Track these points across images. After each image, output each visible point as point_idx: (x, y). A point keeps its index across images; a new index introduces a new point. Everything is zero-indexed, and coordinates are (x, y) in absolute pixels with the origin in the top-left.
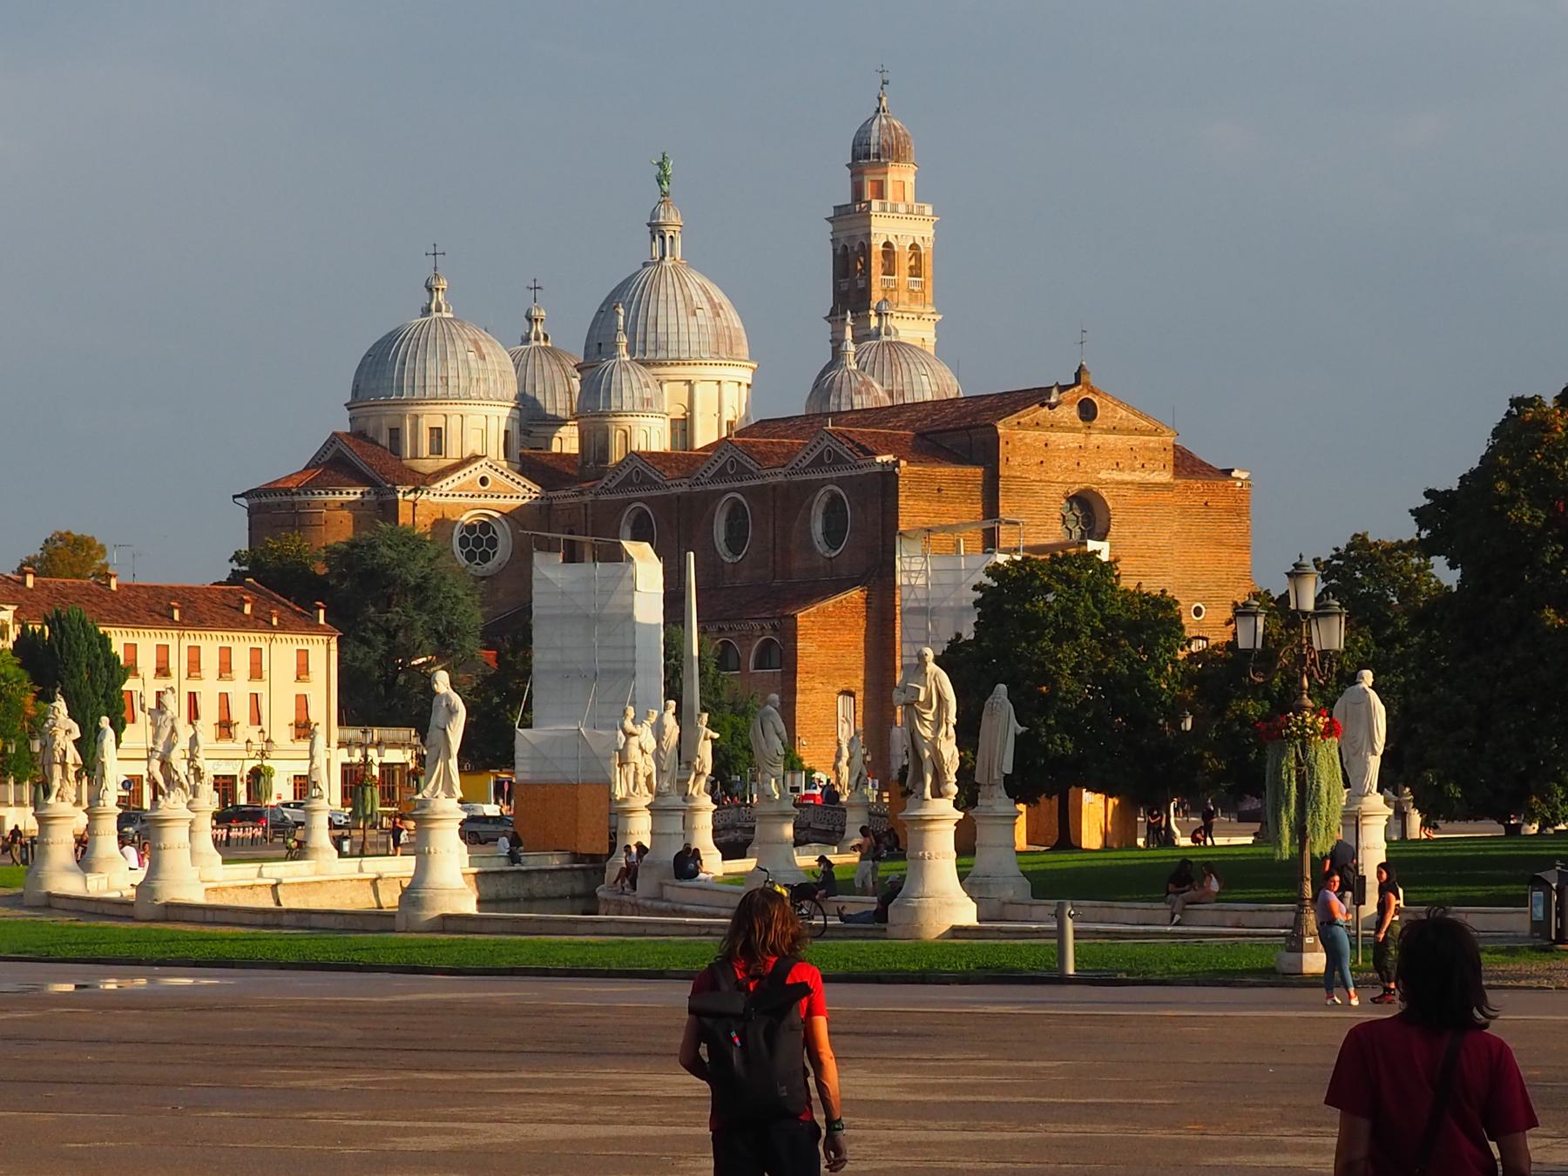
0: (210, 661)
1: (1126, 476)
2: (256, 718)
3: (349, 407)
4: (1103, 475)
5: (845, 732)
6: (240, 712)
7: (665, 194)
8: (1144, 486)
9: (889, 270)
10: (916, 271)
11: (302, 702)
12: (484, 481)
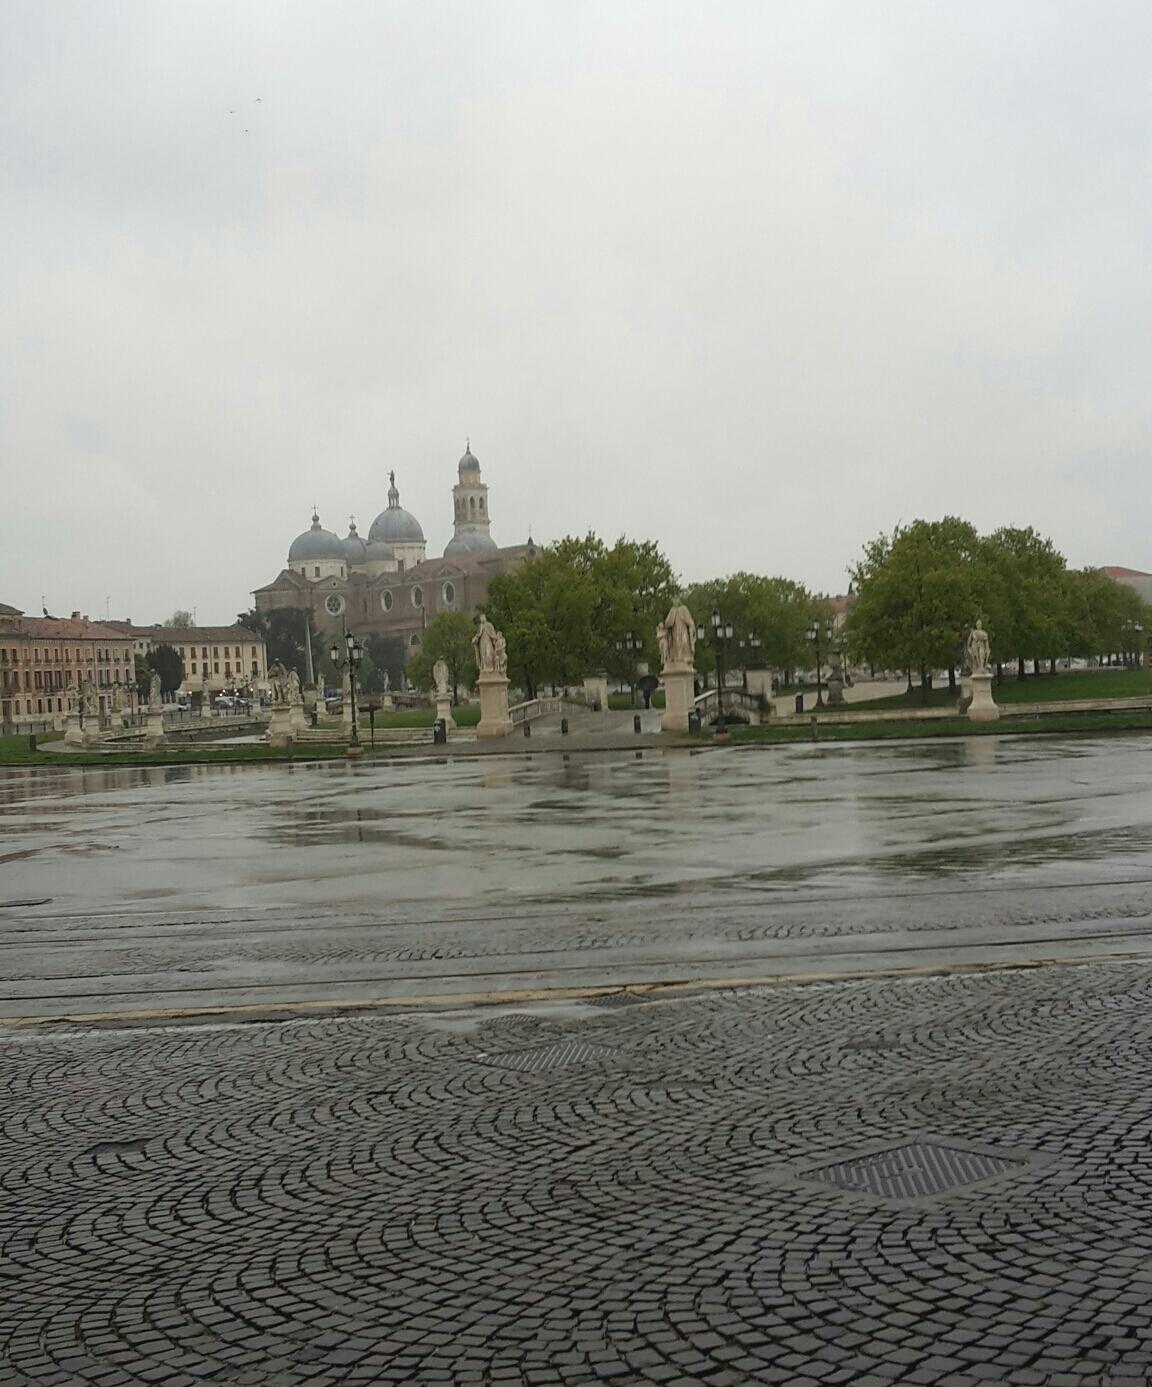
0: (221, 652)
2: (238, 671)
6: (233, 668)
10: (481, 506)
11: (255, 663)
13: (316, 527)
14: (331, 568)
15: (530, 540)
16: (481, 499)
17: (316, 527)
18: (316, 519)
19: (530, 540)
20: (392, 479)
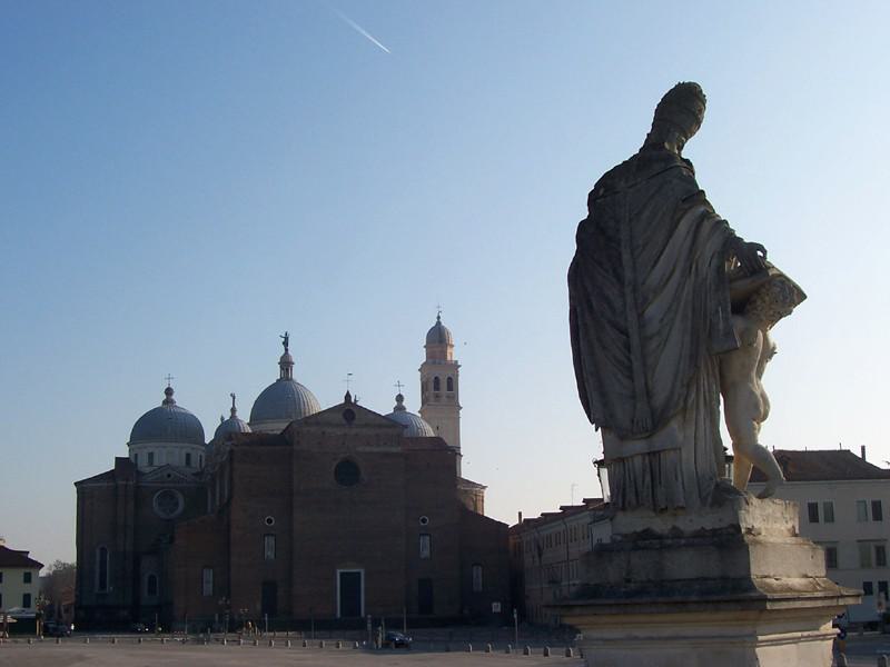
1: (375, 449)
3: (128, 444)
4: (360, 449)
5: (208, 588)
7: (286, 350)
8: (387, 455)
9: (437, 387)
12: (169, 476)
13: (168, 402)
14: (169, 455)
15: (348, 396)
16: (450, 379)
17: (168, 402)
18: (169, 392)
19: (348, 396)
20: (286, 343)
